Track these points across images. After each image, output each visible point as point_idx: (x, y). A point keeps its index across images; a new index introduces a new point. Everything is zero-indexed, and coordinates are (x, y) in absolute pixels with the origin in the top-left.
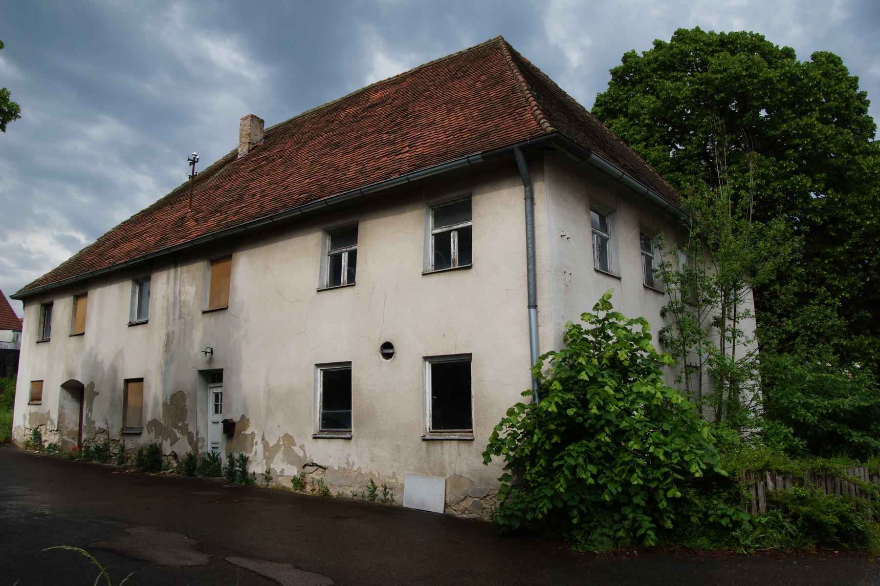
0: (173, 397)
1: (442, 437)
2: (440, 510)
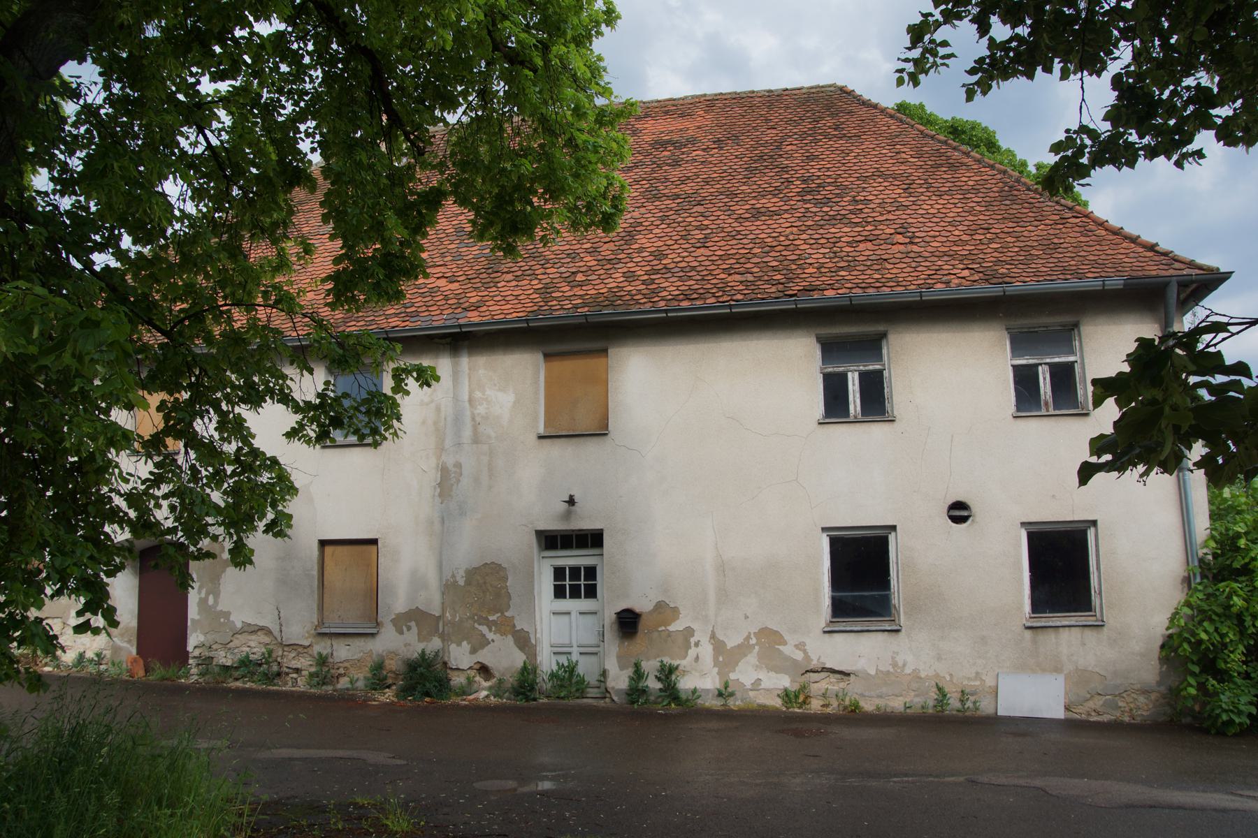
0: (471, 573)
1: (1058, 624)
2: (1060, 714)
